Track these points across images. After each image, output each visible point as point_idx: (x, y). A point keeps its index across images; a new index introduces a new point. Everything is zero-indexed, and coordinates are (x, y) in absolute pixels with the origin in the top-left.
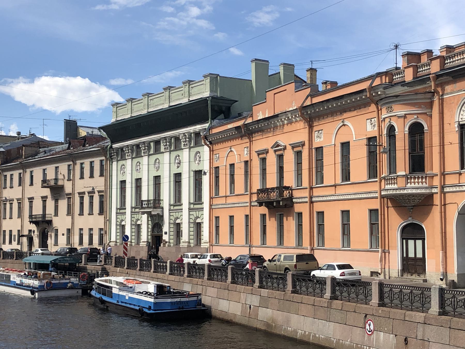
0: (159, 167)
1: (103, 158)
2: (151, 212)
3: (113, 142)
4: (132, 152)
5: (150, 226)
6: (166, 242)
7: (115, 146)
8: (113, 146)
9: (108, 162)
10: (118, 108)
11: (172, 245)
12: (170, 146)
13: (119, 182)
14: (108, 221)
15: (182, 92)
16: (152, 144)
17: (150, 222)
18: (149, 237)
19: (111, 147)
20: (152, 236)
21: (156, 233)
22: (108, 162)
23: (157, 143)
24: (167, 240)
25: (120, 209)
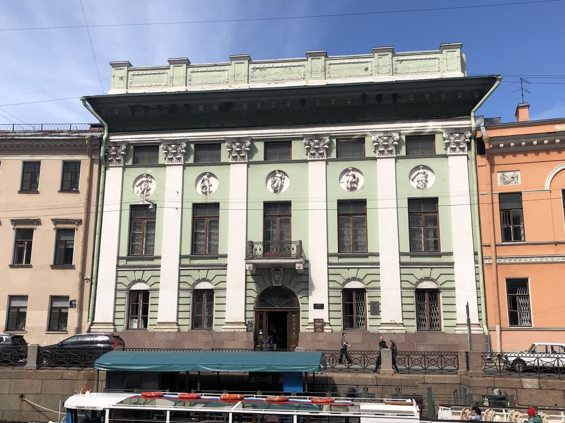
0: (282, 186)
1: (84, 160)
2: (294, 264)
3: (112, 131)
4: (186, 156)
5: (254, 294)
6: (325, 323)
7: (115, 138)
8: (111, 138)
9: (96, 167)
10: (131, 73)
11: (340, 329)
12: (328, 151)
13: (127, 208)
14: (89, 281)
15: (369, 65)
16: (260, 146)
17: (253, 286)
18: (251, 314)
19: (107, 139)
20: (259, 314)
21: (277, 307)
22: (96, 167)
23: (286, 143)
24: (326, 320)
25: (128, 259)
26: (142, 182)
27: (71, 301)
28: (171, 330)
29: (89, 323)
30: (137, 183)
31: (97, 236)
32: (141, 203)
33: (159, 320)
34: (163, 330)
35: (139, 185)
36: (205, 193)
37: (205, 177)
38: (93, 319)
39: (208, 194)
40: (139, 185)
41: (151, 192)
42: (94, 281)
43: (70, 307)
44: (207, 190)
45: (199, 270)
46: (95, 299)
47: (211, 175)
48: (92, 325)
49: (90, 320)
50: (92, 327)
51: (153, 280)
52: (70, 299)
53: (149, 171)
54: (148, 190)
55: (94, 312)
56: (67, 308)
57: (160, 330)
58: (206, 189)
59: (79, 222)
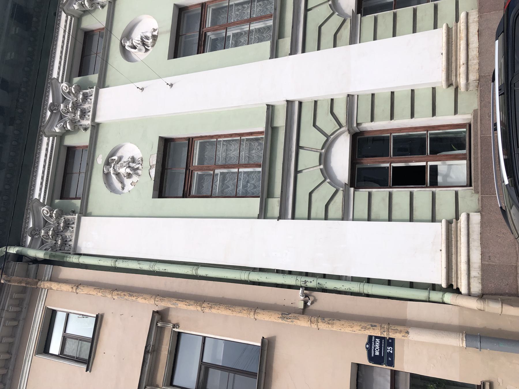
26: (118, 174)
27: (371, 358)
28: (474, 29)
29: (448, 297)
30: (118, 185)
31: (202, 272)
32: (153, 172)
33: (439, 77)
34: (474, 52)
35: (122, 182)
36: (155, 37)
37: (128, 44)
38: (434, 287)
39: (155, 33)
40: (122, 182)
41: (138, 154)
42: (312, 283)
43: (391, 363)
44: (149, 35)
45: (307, 10)
46: (369, 281)
47: (128, 35)
48: (458, 291)
49: (435, 296)
50: (464, 289)
51: (326, 122)
52: (364, 361)
53: (100, 160)
54: (133, 160)
55: (412, 285)
56: (394, 374)
57: (474, 63)
58: (147, 38)
59: (160, 316)
